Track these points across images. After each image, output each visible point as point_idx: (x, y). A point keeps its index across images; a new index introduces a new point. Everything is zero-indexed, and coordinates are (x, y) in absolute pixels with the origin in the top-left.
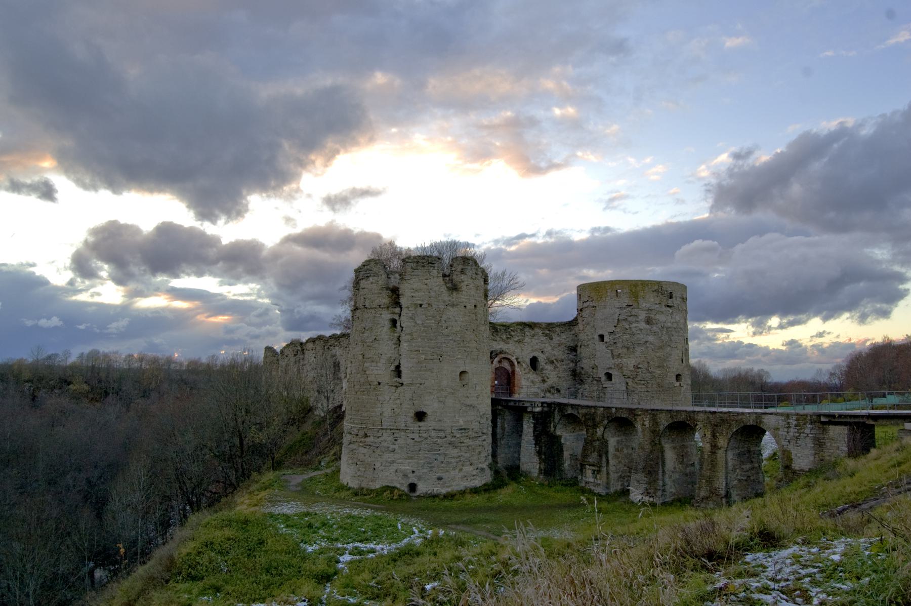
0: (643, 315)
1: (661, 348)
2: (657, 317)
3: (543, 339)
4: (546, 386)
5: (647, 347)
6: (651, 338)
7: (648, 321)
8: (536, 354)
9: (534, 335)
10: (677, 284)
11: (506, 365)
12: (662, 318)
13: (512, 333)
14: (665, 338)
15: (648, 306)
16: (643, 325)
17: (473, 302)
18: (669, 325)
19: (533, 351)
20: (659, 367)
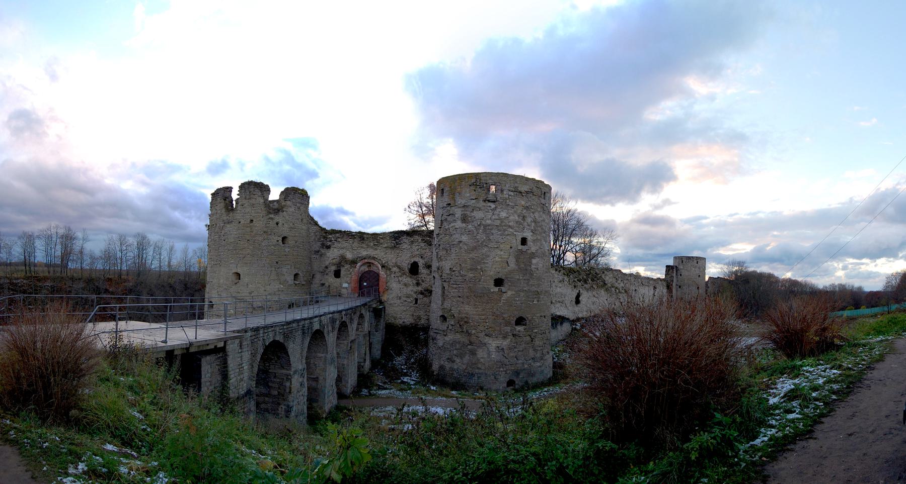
0: (458, 212)
1: (475, 248)
2: (475, 214)
3: (423, 245)
4: (420, 288)
5: (461, 248)
6: (464, 238)
7: (464, 219)
8: (416, 259)
9: (412, 242)
10: (506, 175)
11: (373, 268)
12: (478, 215)
13: (382, 241)
14: (481, 236)
15: (463, 202)
16: (459, 224)
17: (248, 218)
18: (489, 222)
19: (413, 257)
20: (471, 270)
